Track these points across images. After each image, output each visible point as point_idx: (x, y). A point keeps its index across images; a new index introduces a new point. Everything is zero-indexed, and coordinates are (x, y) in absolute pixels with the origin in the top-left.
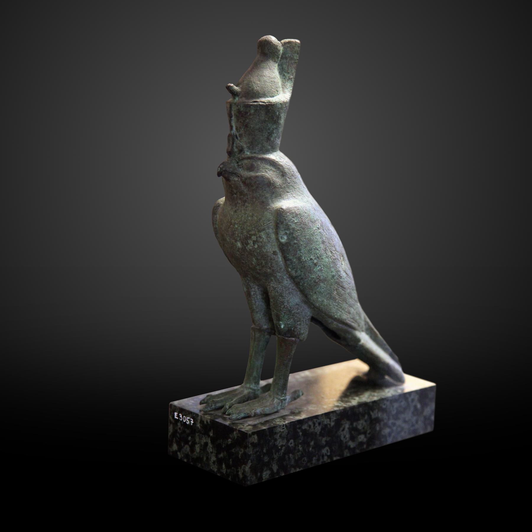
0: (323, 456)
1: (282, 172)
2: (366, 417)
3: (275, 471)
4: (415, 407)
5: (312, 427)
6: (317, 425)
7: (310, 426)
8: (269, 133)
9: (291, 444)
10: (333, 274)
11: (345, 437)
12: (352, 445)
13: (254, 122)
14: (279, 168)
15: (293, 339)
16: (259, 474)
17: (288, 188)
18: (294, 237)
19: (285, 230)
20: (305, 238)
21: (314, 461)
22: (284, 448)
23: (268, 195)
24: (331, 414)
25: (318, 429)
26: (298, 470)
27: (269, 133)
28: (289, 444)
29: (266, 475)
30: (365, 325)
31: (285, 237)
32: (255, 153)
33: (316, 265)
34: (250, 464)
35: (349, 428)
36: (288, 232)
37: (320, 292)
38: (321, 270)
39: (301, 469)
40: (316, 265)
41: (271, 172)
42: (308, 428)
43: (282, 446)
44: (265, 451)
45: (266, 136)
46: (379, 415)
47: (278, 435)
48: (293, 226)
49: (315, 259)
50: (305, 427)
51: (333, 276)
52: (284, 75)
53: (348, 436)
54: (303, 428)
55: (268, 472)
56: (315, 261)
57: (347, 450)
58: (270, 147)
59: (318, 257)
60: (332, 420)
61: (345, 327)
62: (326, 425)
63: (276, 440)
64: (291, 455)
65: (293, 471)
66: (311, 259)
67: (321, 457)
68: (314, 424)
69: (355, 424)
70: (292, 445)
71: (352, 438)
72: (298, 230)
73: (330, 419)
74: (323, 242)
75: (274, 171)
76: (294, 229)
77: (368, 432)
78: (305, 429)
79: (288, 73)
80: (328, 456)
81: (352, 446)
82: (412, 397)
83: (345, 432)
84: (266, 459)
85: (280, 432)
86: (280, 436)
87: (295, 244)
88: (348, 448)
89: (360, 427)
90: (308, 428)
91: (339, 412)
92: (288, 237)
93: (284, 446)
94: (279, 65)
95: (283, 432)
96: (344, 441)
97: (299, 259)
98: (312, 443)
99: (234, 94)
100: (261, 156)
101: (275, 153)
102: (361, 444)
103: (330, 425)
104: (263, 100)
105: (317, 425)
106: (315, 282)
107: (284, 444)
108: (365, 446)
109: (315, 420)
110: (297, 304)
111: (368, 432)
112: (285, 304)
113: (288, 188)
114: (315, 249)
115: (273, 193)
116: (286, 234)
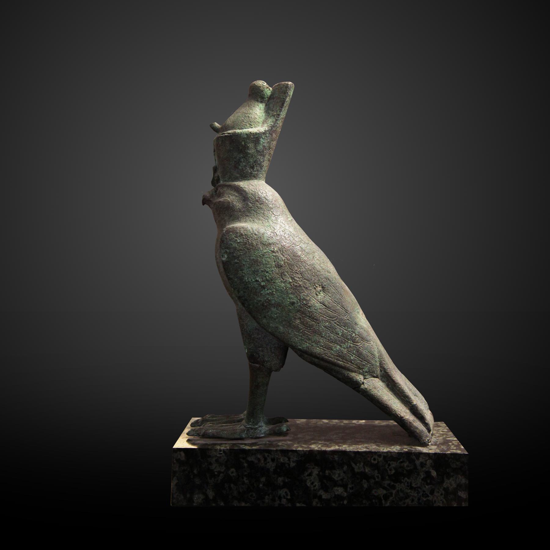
0: (280, 498)
1: (244, 197)
2: (345, 468)
3: (211, 497)
4: (428, 473)
5: (262, 462)
6: (269, 460)
7: (259, 460)
8: (235, 162)
9: (232, 473)
10: (292, 300)
11: (312, 483)
12: (325, 496)
13: (235, 156)
14: (242, 194)
15: (257, 365)
16: (188, 496)
17: (249, 212)
18: (234, 256)
19: (225, 248)
20: (249, 259)
21: (267, 499)
22: (221, 475)
23: (226, 218)
24: (290, 453)
25: (271, 466)
26: (243, 504)
27: (235, 162)
28: (230, 472)
29: (198, 498)
30: (381, 371)
31: (226, 256)
32: (225, 181)
33: (263, 287)
34: (177, 481)
35: (318, 475)
36: (228, 251)
37: (271, 318)
38: (272, 294)
39: (248, 505)
40: (264, 288)
41: (234, 197)
42: (256, 461)
43: (220, 472)
44: (195, 472)
45: (233, 164)
46: (367, 470)
47: (214, 459)
48: (235, 245)
49: (262, 281)
50: (251, 459)
51: (293, 303)
52: (269, 113)
53: (317, 484)
54: (250, 459)
55: (202, 497)
56: (263, 284)
57: (317, 500)
58: (238, 175)
59: (267, 280)
60: (291, 460)
61: (326, 364)
62: (283, 464)
63: (211, 464)
64: (232, 485)
65: (236, 503)
66: (257, 281)
67: (277, 498)
68: (265, 459)
69: (327, 472)
70: (234, 474)
71: (325, 488)
72: (241, 250)
73: (289, 459)
74: (279, 266)
75: (237, 196)
76: (235, 248)
77: (350, 486)
78: (252, 462)
79: (273, 111)
80: (287, 499)
81: (324, 497)
82: (421, 460)
83: (312, 478)
84: (197, 481)
85: (216, 456)
86: (217, 461)
87: (237, 263)
88: (320, 497)
89: (336, 477)
90: (256, 461)
91: (302, 453)
92: (228, 255)
93: (223, 473)
94: (266, 105)
95: (220, 457)
96: (312, 489)
97: (241, 279)
98: (263, 479)
99: (216, 130)
100: (228, 183)
101: (246, 181)
102: (339, 498)
103: (289, 465)
104: (230, 132)
105: (269, 460)
106: (263, 305)
107: (222, 470)
108: (345, 502)
109: (266, 455)
110: (256, 329)
111: (350, 486)
112: (245, 328)
113: (249, 212)
114: (262, 271)
115: (231, 216)
116: (226, 252)
